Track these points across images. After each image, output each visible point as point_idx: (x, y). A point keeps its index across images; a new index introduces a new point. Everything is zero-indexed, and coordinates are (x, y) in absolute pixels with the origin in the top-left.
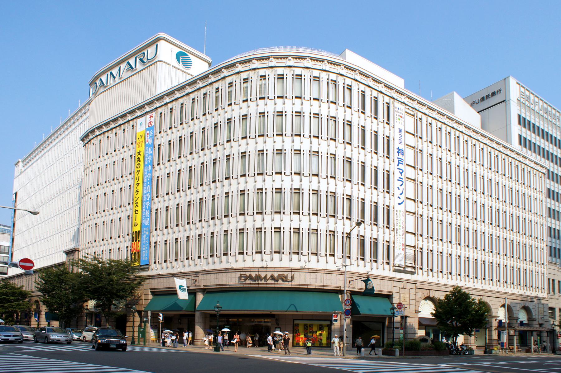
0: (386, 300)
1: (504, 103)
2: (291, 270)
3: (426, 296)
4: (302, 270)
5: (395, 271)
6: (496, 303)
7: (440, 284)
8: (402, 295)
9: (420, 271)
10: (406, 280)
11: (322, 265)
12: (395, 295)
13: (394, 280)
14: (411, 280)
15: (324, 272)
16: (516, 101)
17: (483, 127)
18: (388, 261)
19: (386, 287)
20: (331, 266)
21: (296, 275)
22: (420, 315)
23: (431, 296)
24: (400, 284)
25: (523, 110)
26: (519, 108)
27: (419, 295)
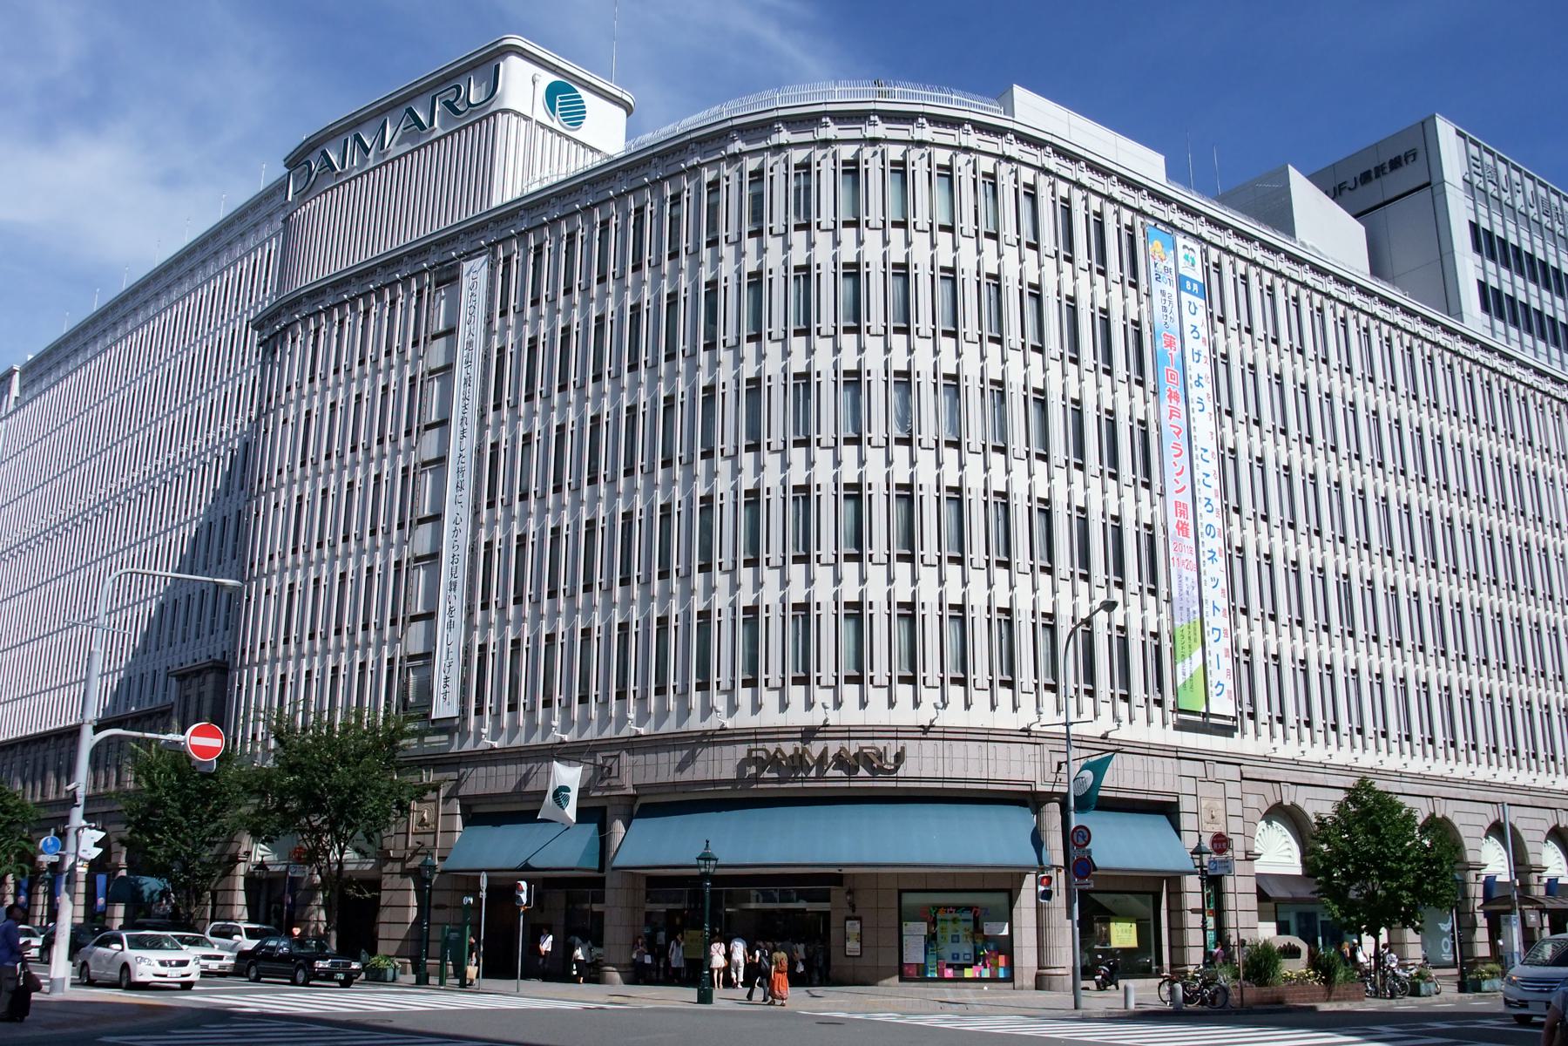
0: (1162, 820)
1: (1427, 191)
2: (896, 733)
3: (1272, 802)
4: (926, 731)
5: (1181, 726)
6: (1471, 819)
7: (1309, 764)
8: (1204, 803)
9: (1249, 724)
10: (1213, 753)
11: (980, 717)
12: (1186, 804)
13: (1178, 754)
14: (1227, 754)
15: (987, 736)
16: (1460, 184)
17: (1376, 270)
18: (1159, 697)
19: (1158, 778)
20: (1005, 719)
21: (911, 747)
22: (1260, 867)
23: (1286, 803)
24: (1196, 769)
25: (1482, 210)
26: (1471, 204)
27: (1252, 801)
